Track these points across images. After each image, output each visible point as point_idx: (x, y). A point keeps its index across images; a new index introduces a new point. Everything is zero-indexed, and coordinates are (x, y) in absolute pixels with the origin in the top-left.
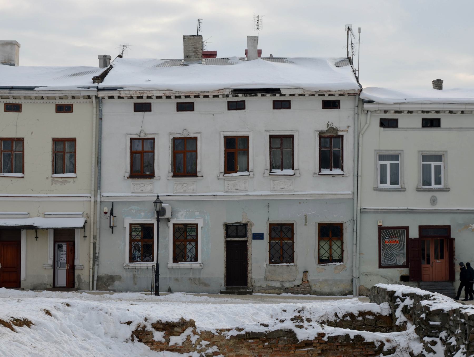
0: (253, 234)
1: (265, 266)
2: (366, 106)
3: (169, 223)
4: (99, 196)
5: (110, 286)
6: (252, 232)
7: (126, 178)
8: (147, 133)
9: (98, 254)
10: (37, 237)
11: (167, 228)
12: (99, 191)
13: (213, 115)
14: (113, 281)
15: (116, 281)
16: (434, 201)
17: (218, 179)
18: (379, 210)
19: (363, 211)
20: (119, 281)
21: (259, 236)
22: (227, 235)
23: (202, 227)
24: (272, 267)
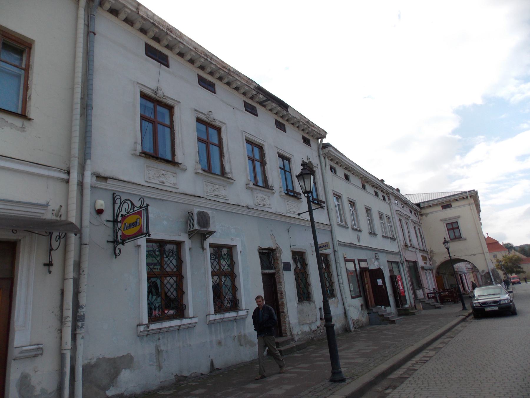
1: (296, 305)
3: (205, 242)
5: (112, 388)
6: (283, 261)
7: (139, 154)
9: (83, 310)
11: (201, 250)
12: (88, 162)
13: (234, 109)
14: (117, 374)
15: (123, 370)
16: (359, 240)
18: (344, 244)
20: (129, 368)
21: (287, 267)
23: (241, 251)
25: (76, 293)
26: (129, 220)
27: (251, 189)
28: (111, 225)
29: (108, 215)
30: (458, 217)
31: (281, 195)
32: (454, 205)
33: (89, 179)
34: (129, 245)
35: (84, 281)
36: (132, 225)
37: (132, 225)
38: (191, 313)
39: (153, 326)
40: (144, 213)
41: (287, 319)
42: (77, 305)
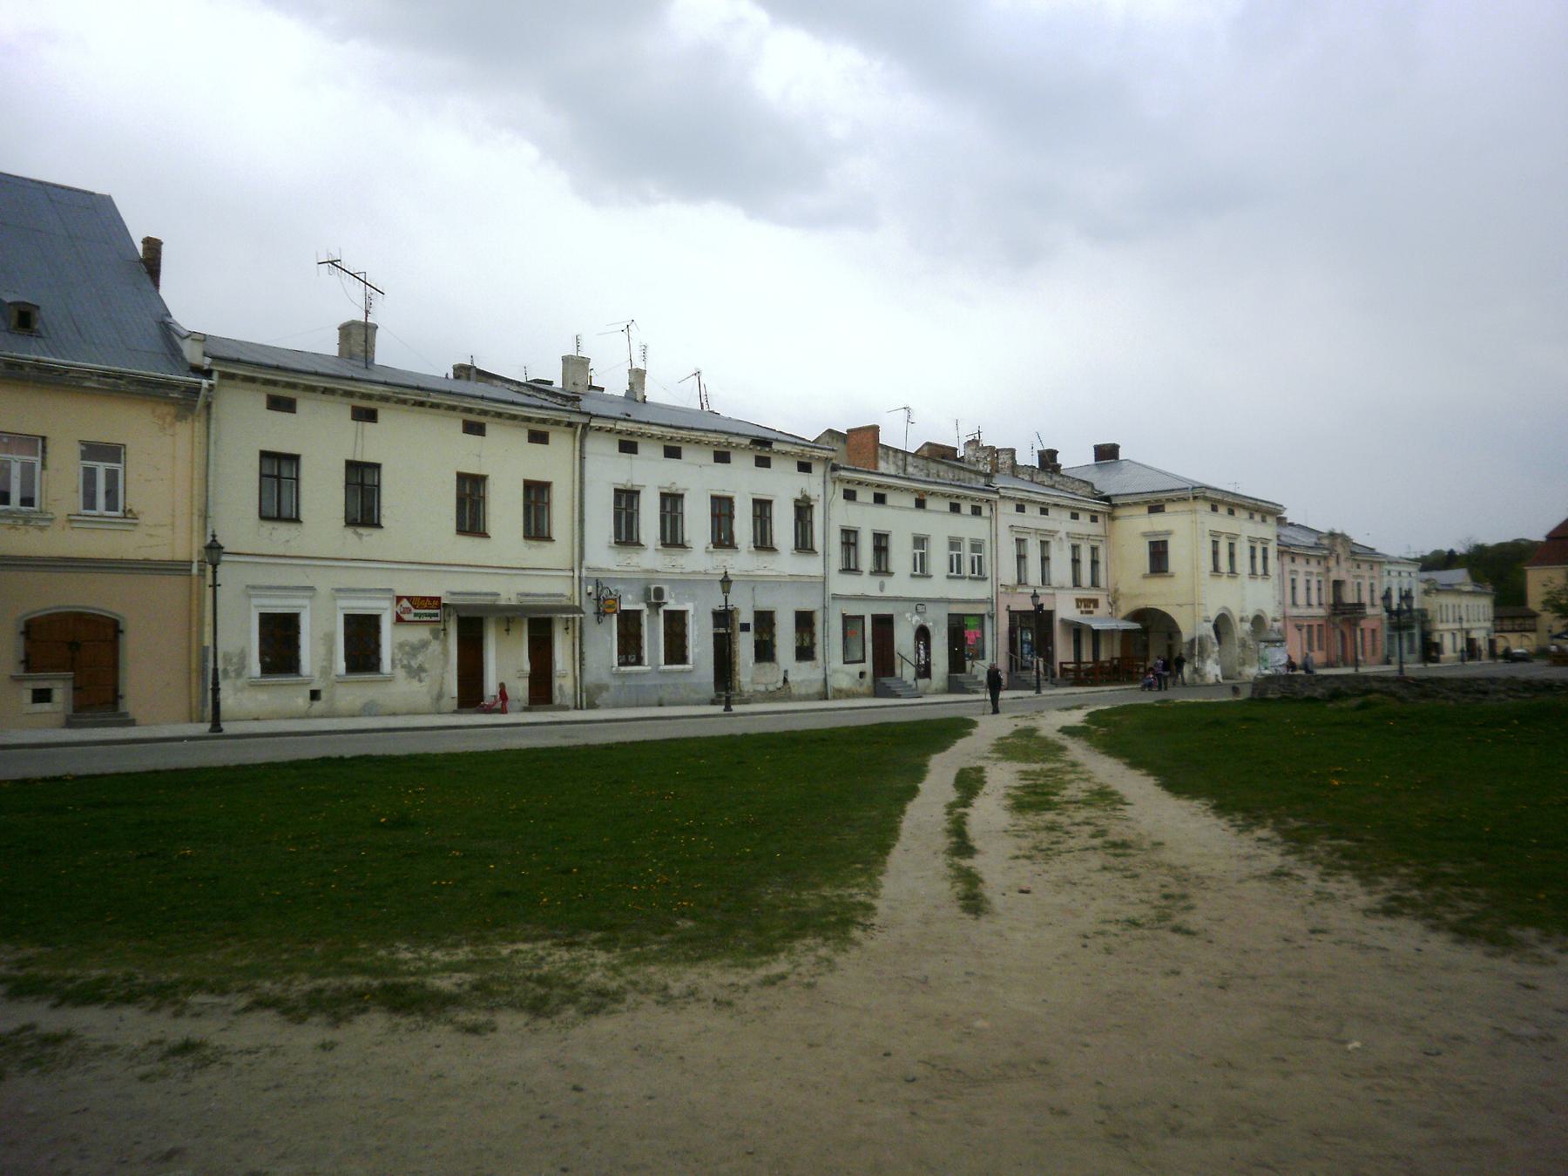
0: (741, 624)
1: (751, 665)
2: (843, 473)
4: (583, 570)
6: (740, 622)
8: (634, 483)
10: (508, 630)
16: (882, 588)
17: (706, 552)
19: (835, 597)
21: (745, 627)
22: (715, 626)
24: (757, 665)
25: (581, 645)
26: (611, 602)
27: (712, 552)
28: (595, 602)
29: (594, 596)
30: (1169, 533)
31: (749, 552)
32: (1168, 508)
33: (584, 573)
34: (607, 617)
35: (585, 638)
36: (610, 607)
37: (610, 607)
38: (646, 661)
39: (623, 668)
40: (618, 601)
41: (738, 677)
42: (581, 653)
